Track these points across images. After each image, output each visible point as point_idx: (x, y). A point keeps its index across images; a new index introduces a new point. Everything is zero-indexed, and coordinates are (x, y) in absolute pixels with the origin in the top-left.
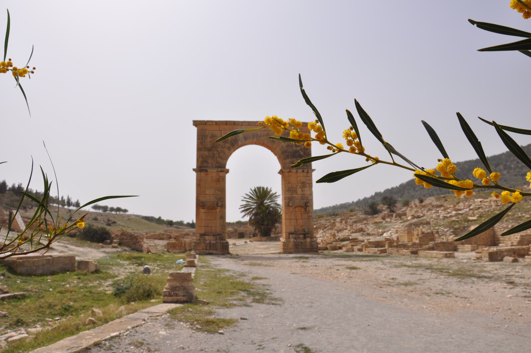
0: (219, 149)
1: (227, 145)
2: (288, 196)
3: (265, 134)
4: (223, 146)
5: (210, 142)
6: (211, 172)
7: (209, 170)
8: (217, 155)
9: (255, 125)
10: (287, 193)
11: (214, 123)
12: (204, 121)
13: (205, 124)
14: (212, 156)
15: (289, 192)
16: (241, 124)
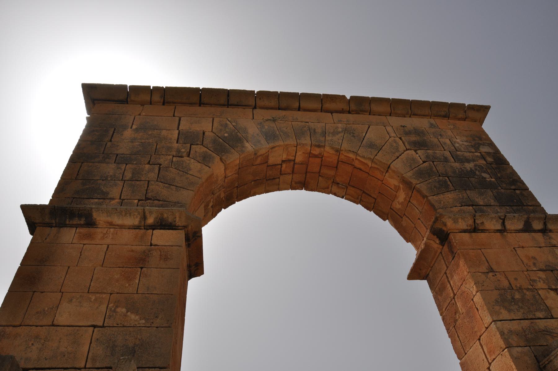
0: (164, 160)
1: (198, 149)
2: (515, 326)
3: (340, 130)
4: (178, 151)
5: (133, 140)
6: (111, 225)
7: (100, 218)
8: (153, 176)
9: (299, 109)
10: (505, 314)
11: (156, 98)
12: (122, 88)
13: (125, 101)
14: (128, 175)
15: (509, 311)
16: (252, 102)
